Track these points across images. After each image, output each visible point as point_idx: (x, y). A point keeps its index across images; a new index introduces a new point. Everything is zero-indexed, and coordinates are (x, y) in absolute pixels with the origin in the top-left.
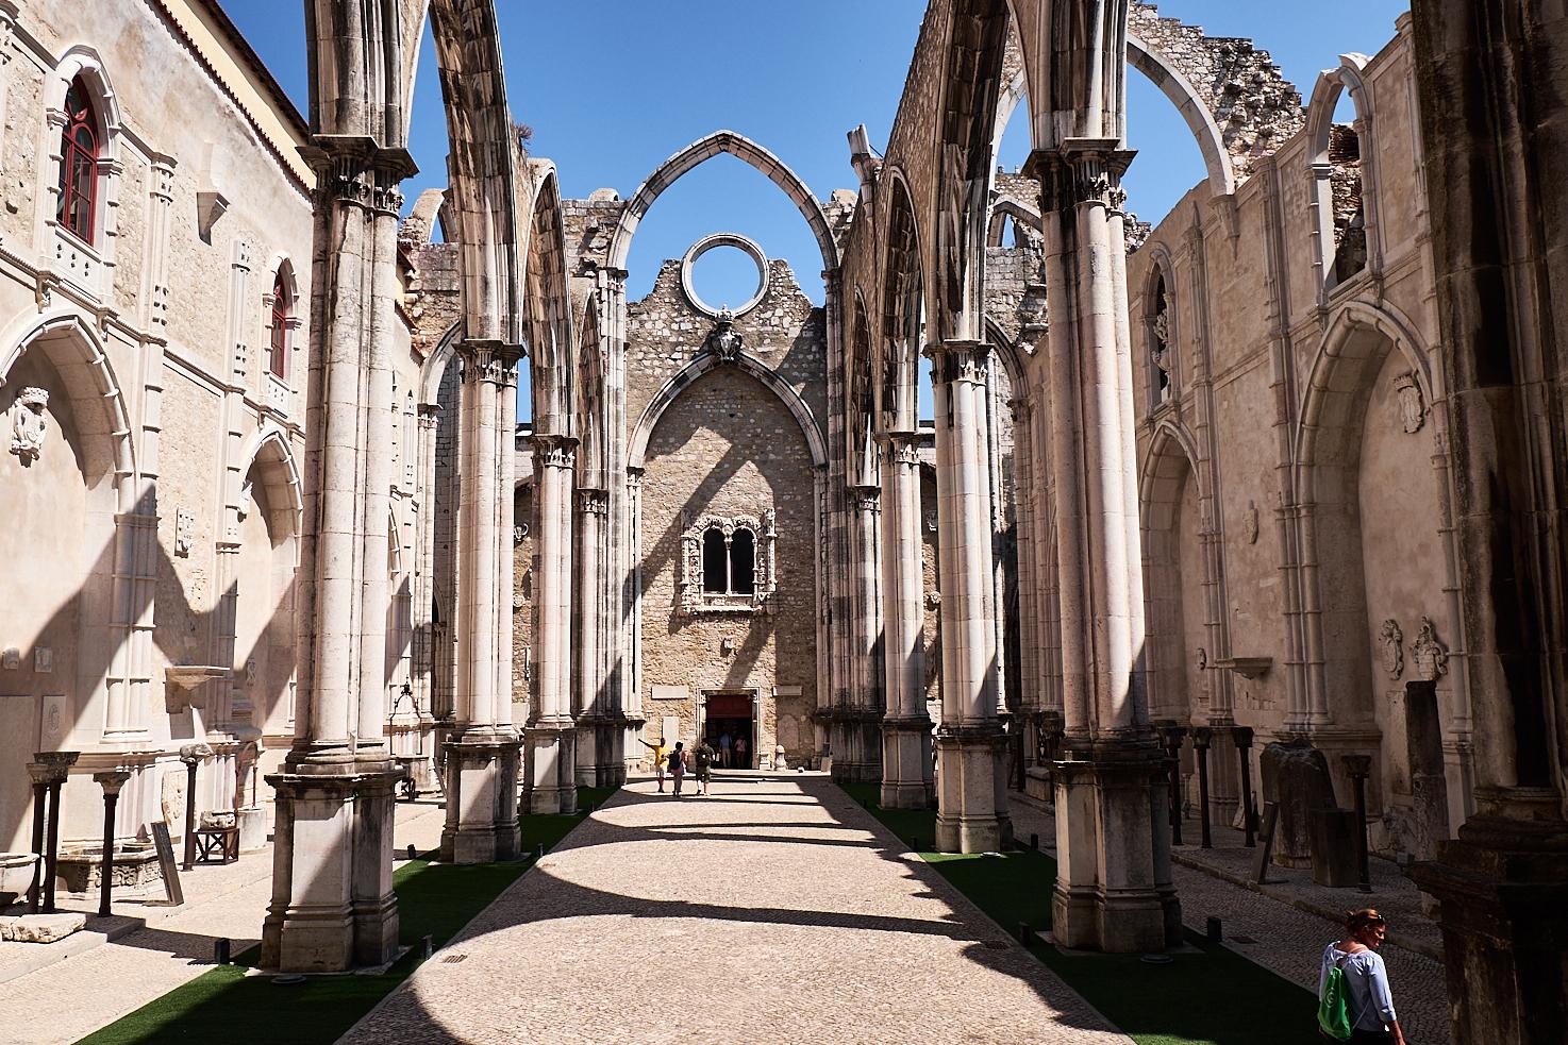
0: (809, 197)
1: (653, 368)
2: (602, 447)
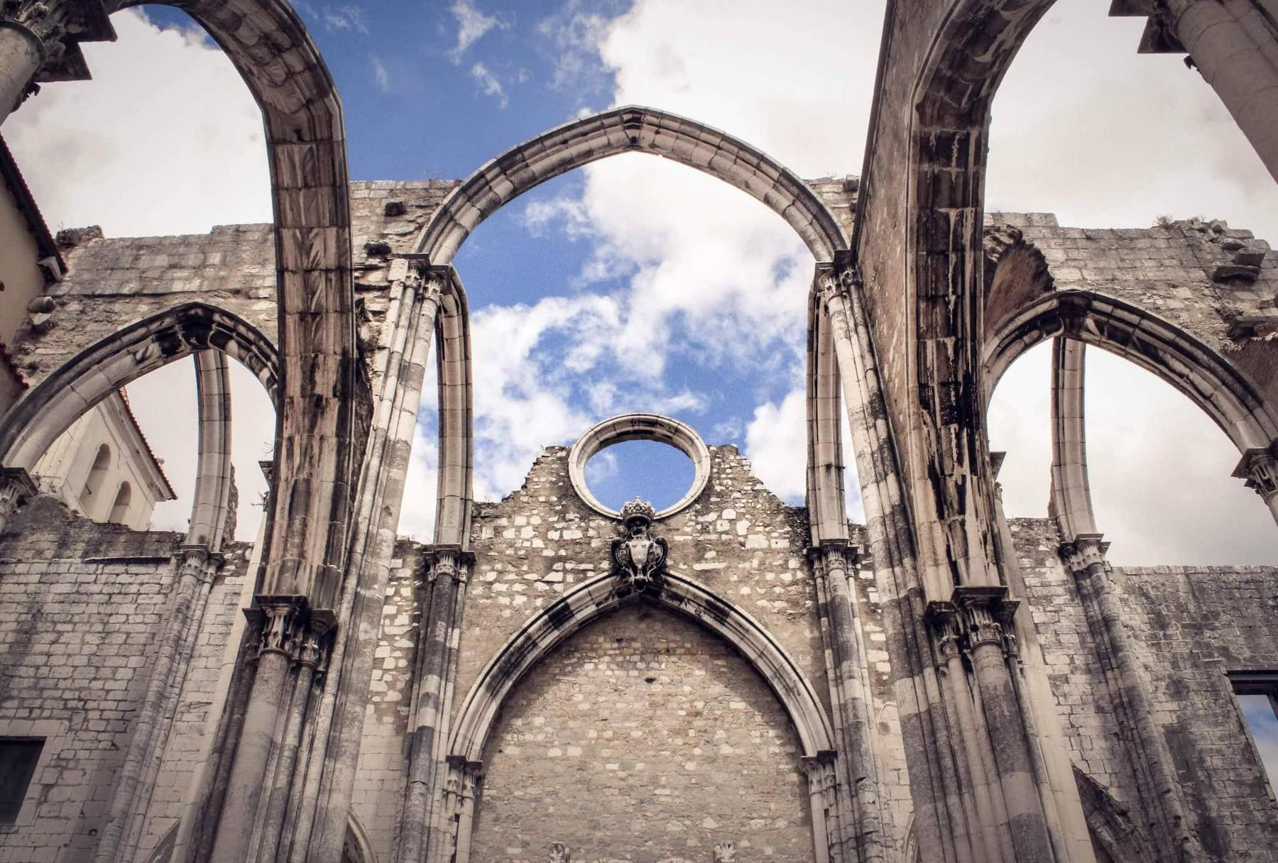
1: (511, 595)
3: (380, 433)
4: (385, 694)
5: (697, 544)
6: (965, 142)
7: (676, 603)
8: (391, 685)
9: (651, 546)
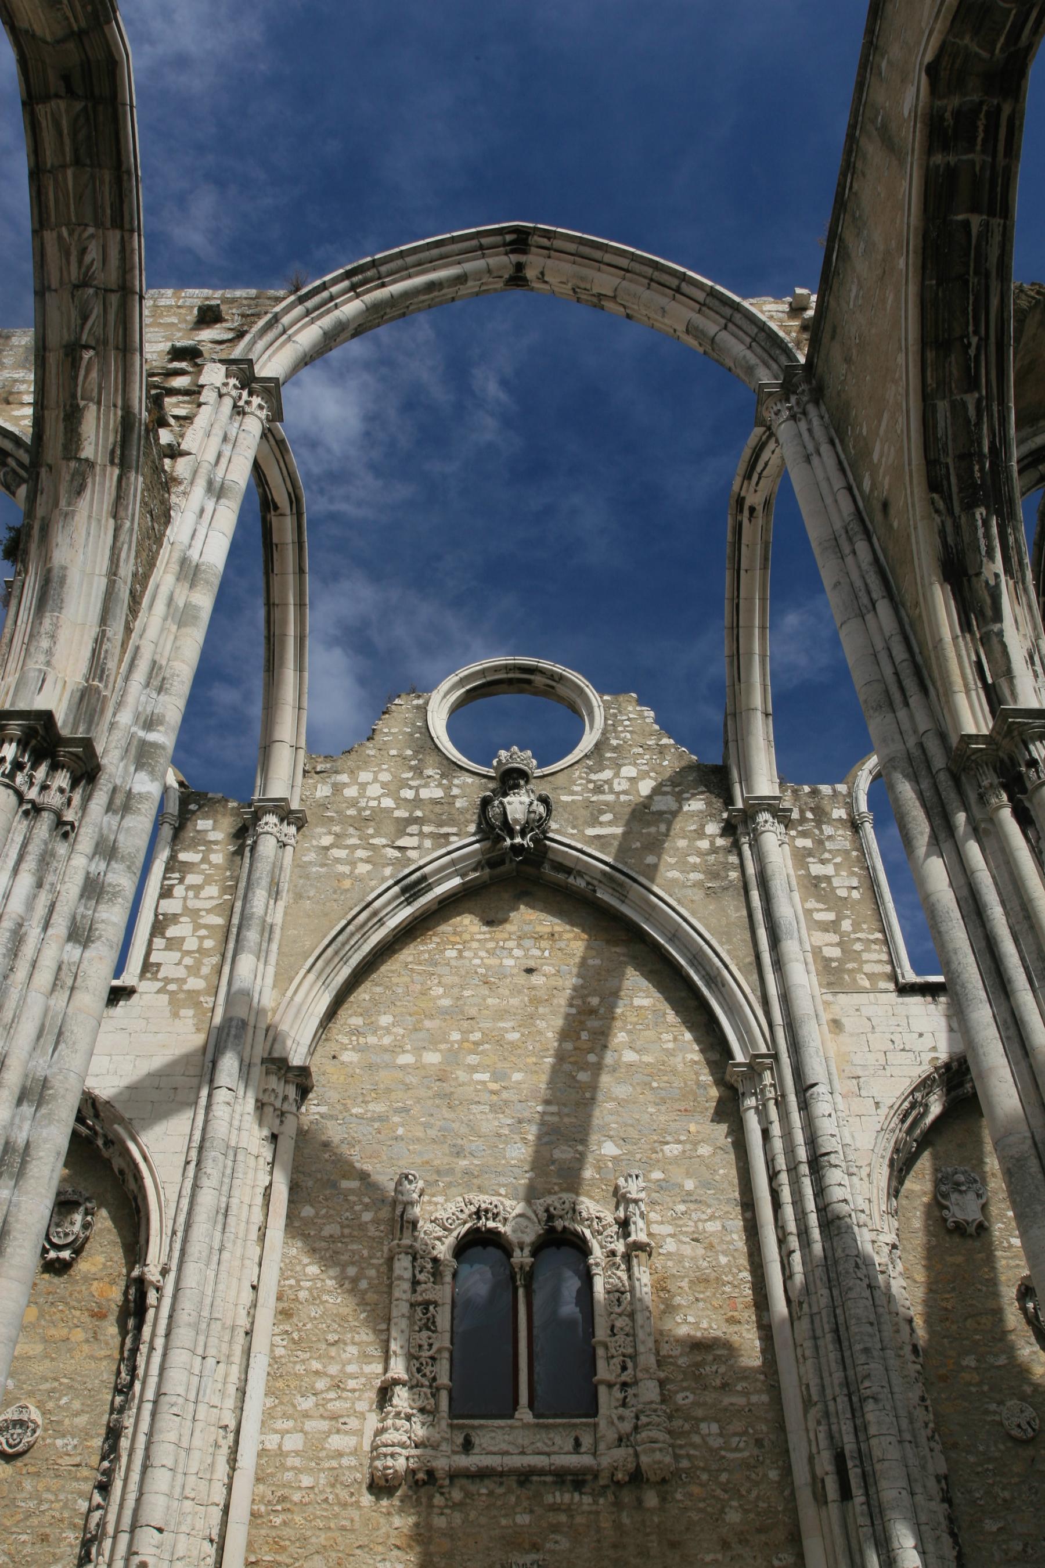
0: (712, 293)
3: (178, 547)
4: (183, 981)
5: (588, 804)
6: (994, 115)
7: (561, 876)
8: (194, 970)
9: (531, 803)
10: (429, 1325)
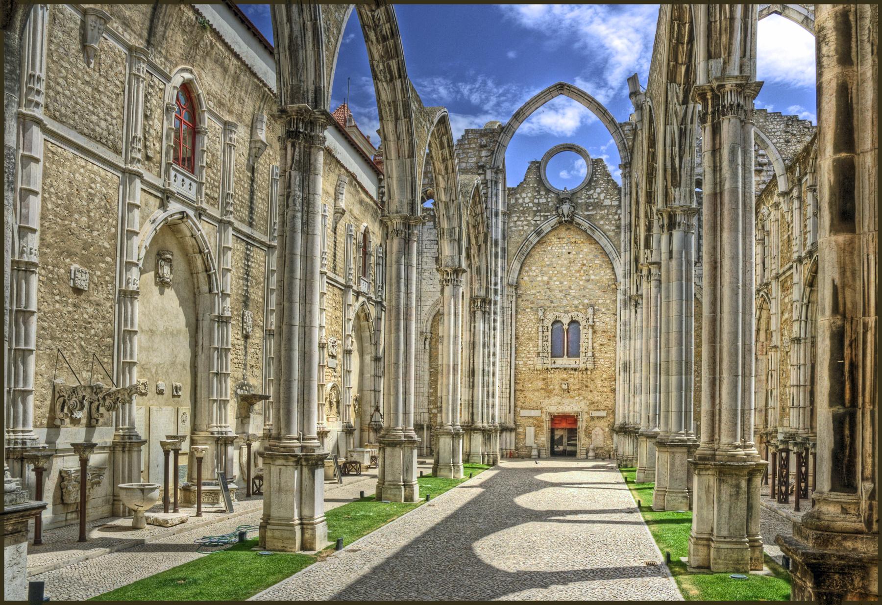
2: (487, 273)
5: (586, 203)
10: (547, 341)
